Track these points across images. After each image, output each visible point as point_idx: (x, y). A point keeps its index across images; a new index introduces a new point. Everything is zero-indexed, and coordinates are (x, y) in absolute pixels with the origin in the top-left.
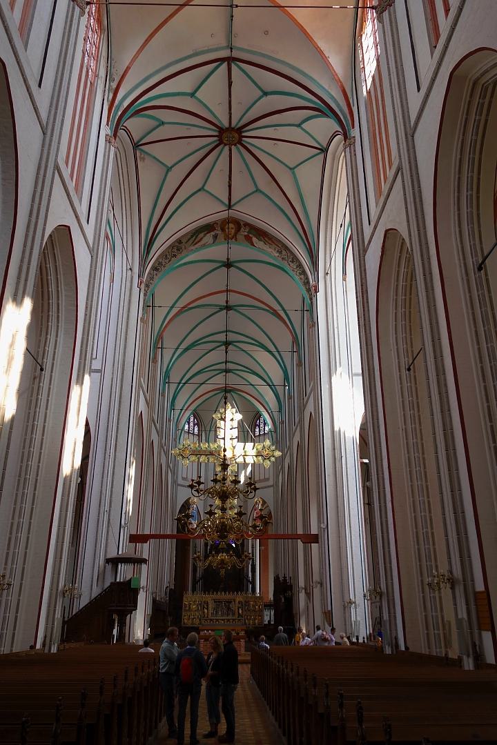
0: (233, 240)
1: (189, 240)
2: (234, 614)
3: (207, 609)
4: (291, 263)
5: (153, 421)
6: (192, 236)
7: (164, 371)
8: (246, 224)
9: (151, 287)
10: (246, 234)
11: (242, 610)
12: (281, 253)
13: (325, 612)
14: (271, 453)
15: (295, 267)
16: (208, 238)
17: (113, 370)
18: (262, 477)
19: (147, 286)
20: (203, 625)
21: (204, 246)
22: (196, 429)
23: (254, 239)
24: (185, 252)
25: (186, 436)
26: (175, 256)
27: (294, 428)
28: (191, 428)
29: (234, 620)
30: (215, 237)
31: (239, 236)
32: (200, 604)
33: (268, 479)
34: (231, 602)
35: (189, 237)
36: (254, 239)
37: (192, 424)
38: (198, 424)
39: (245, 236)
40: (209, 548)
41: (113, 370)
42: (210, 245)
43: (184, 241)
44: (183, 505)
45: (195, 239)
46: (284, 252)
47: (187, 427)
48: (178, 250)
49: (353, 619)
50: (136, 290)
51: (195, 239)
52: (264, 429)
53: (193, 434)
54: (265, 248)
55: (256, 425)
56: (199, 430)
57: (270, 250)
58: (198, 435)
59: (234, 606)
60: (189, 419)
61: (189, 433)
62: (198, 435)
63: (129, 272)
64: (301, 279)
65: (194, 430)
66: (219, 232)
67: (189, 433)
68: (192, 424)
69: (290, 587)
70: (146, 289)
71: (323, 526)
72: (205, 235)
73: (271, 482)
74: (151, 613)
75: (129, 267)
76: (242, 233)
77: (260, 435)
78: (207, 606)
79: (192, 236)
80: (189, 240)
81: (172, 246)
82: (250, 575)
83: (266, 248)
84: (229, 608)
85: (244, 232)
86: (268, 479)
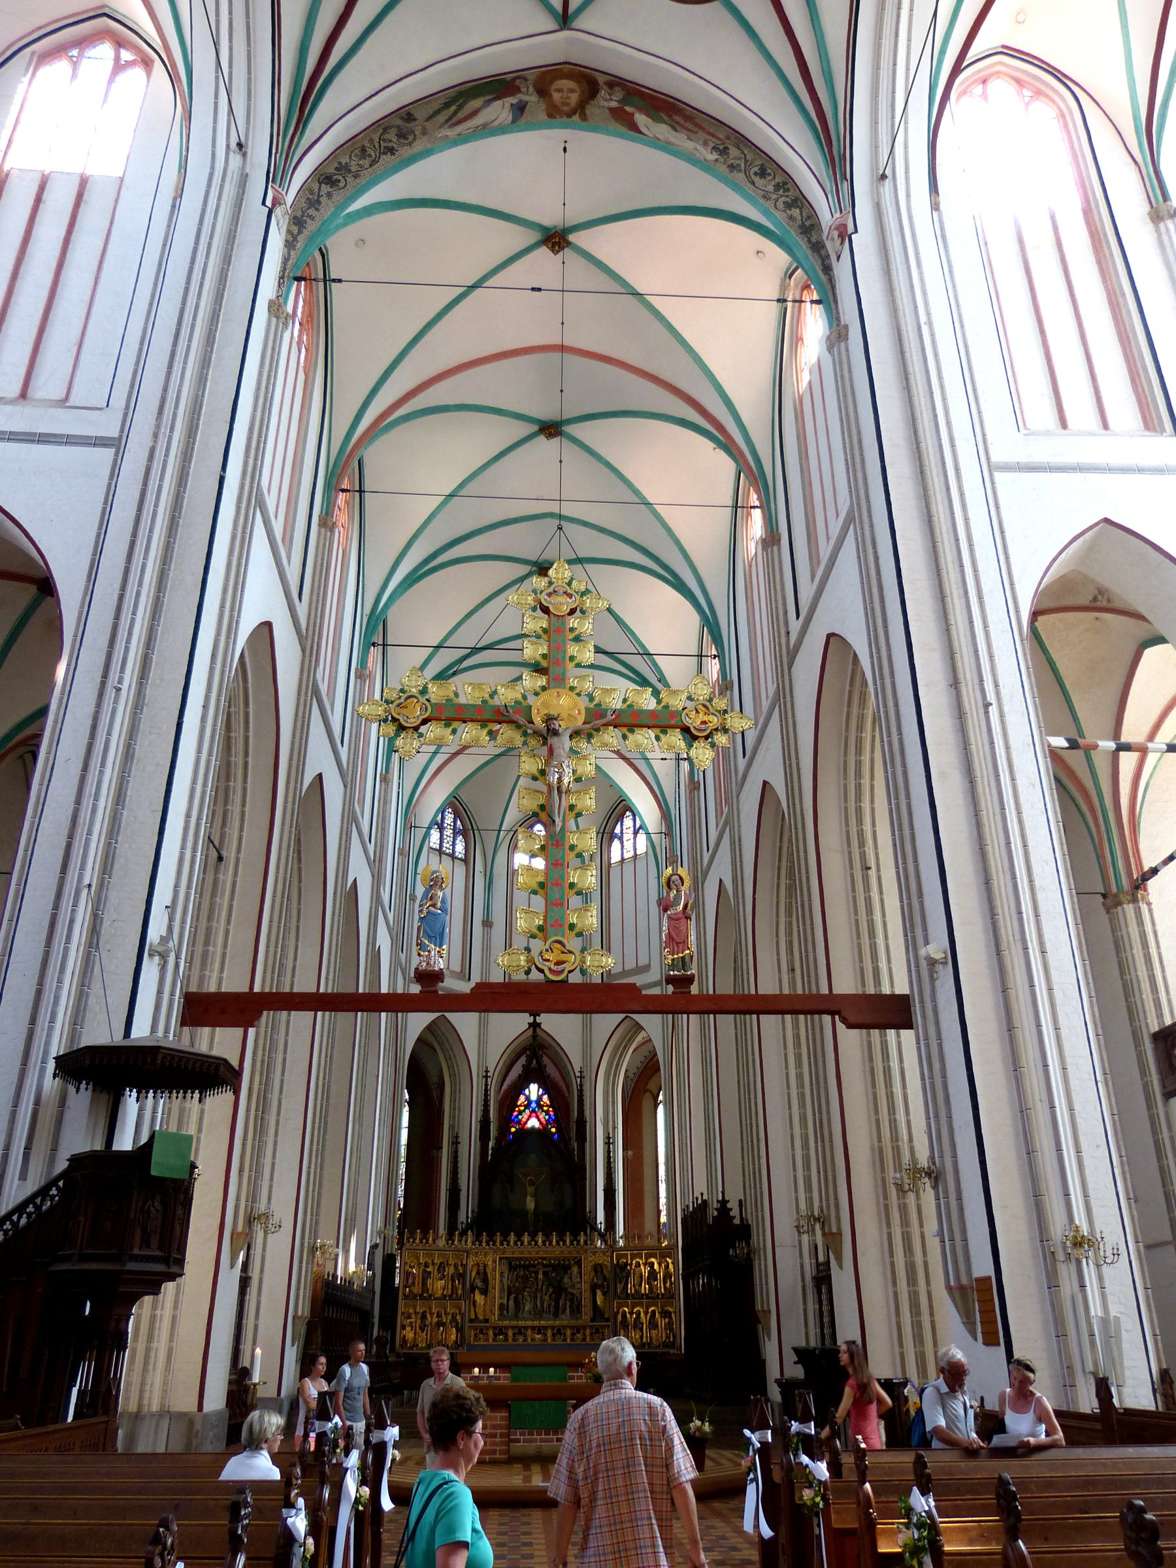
0: (576, 118)
1: (437, 113)
2: (576, 1310)
3: (485, 1292)
4: (757, 179)
5: (316, 693)
6: (447, 105)
7: (367, 610)
8: (616, 82)
9: (311, 226)
10: (614, 104)
11: (605, 1294)
12: (724, 152)
13: (962, 1288)
14: (715, 721)
15: (771, 188)
16: (500, 111)
17: (158, 426)
19: (298, 222)
20: (471, 1348)
21: (487, 130)
22: (460, 848)
23: (641, 119)
24: (418, 146)
25: (435, 858)
26: (391, 151)
27: (742, 763)
28: (447, 846)
29: (578, 1329)
30: (520, 109)
31: (590, 110)
32: (462, 1276)
33: (647, 968)
34: (566, 1268)
35: (436, 106)
36: (641, 119)
38: (464, 833)
39: (612, 110)
40: (491, 1144)
41: (158, 426)
42: (502, 130)
43: (421, 114)
44: (420, 1040)
45: (456, 112)
46: (734, 152)
47: (435, 836)
48: (402, 135)
49: (1096, 1310)
50: (255, 212)
51: (456, 112)
53: (452, 856)
54: (673, 140)
55: (612, 836)
56: (466, 848)
57: (690, 145)
58: (465, 861)
59: (581, 1282)
60: (443, 818)
61: (440, 851)
62: (465, 861)
63: (235, 160)
64: (791, 218)
65: (454, 845)
66: (532, 98)
67: (440, 851)
68: (448, 832)
69: (744, 1231)
70: (295, 229)
71: (936, 948)
72: (487, 103)
74: (307, 1313)
75: (234, 141)
76: (603, 103)
78: (485, 1280)
79: (447, 105)
80: (437, 113)
81: (382, 125)
82: (601, 1216)
83: (680, 139)
84: (559, 1290)
85: (607, 100)
86: (647, 968)
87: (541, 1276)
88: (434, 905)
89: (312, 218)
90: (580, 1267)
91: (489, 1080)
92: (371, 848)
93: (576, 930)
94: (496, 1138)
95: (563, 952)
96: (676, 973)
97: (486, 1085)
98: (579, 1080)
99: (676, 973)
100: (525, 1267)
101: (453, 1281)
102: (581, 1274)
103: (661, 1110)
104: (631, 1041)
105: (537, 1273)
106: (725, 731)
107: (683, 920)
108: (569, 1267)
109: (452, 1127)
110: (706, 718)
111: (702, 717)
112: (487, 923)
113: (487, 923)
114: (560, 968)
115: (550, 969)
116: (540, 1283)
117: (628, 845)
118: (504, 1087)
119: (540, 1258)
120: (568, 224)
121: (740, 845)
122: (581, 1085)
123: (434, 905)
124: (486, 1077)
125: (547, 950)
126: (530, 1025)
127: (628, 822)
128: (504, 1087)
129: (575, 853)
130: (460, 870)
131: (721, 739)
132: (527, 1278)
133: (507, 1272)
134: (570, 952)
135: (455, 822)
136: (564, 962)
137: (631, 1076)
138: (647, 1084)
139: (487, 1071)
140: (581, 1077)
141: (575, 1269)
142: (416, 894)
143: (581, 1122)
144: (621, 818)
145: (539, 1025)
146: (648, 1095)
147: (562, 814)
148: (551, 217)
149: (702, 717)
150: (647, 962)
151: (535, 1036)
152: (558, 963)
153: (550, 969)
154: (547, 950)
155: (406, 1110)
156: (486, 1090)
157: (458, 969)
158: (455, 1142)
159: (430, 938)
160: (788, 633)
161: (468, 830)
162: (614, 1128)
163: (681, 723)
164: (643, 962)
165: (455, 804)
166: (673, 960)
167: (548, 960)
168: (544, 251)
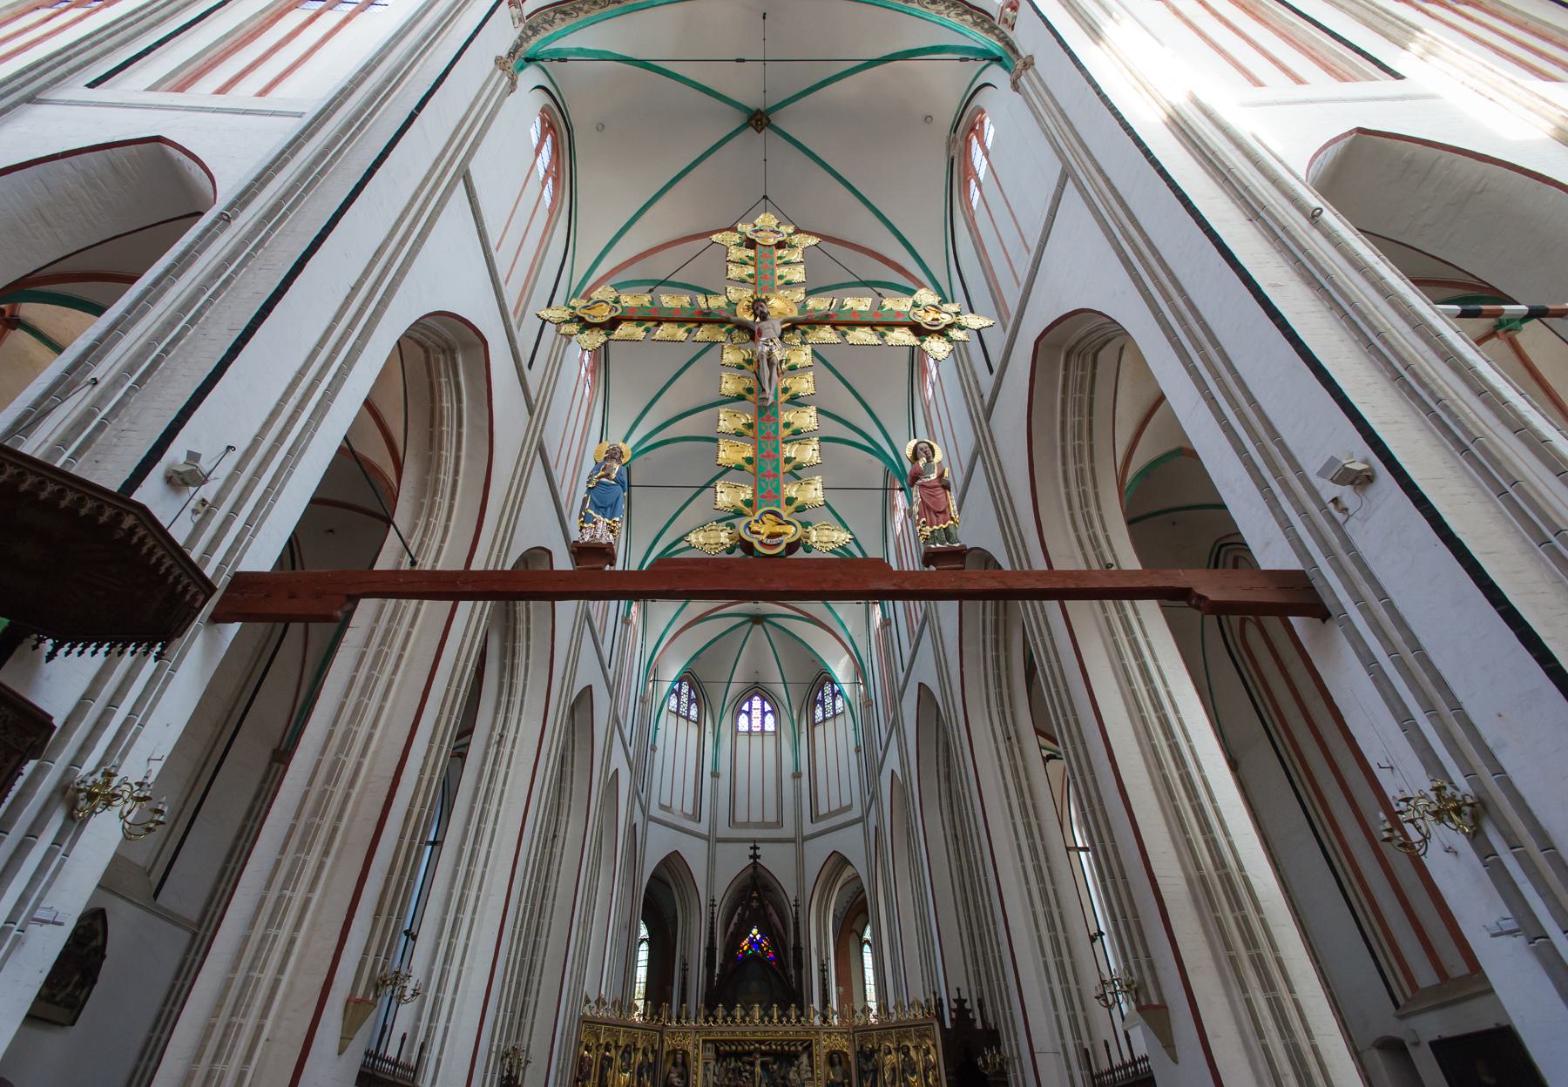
4: (929, 6)
5: (541, 449)
14: (947, 319)
15: (942, 8)
18: (835, 806)
22: (694, 712)
25: (672, 718)
28: (683, 710)
33: (850, 807)
37: (684, 699)
38: (697, 701)
44: (654, 876)
52: (834, 706)
53: (687, 718)
55: (816, 702)
56: (699, 713)
60: (680, 687)
61: (677, 714)
62: (698, 723)
65: (689, 709)
68: (684, 699)
73: (856, 812)
77: (825, 719)
86: (850, 807)
87: (758, 1069)
88: (607, 476)
89: (545, 29)
90: (810, 1056)
91: (716, 909)
92: (611, 672)
93: (796, 504)
94: (721, 965)
95: (779, 524)
96: (938, 545)
97: (713, 913)
98: (794, 909)
99: (938, 545)
100: (738, 1056)
101: (640, 1075)
102: (812, 1066)
103: (867, 948)
104: (839, 874)
105: (752, 1064)
106: (962, 328)
107: (941, 490)
108: (797, 1056)
109: (683, 957)
110: (936, 316)
111: (932, 315)
112: (715, 775)
113: (715, 775)
114: (775, 541)
115: (761, 542)
116: (757, 1080)
117: (829, 707)
118: (729, 933)
119: (757, 1041)
120: (769, 106)
121: (940, 634)
122: (797, 913)
123: (607, 476)
124: (713, 906)
125: (756, 521)
126: (751, 857)
127: (828, 689)
128: (729, 933)
129: (790, 429)
130: (694, 729)
131: (956, 334)
132: (740, 1072)
133: (713, 1063)
134: (789, 523)
135: (690, 692)
136: (779, 535)
137: (839, 915)
138: (852, 924)
139: (713, 900)
140: (796, 906)
141: (804, 1059)
142: (657, 745)
143: (798, 949)
144: (821, 688)
145: (759, 857)
146: (854, 935)
147: (773, 388)
148: (754, 101)
149: (932, 315)
150: (849, 803)
151: (755, 865)
152: (771, 536)
153: (761, 542)
154: (756, 521)
155: (644, 946)
156: (713, 918)
157: (691, 813)
158: (685, 969)
159: (597, 508)
160: (982, 396)
161: (701, 697)
162: (828, 958)
163: (908, 320)
164: (846, 802)
165: (688, 676)
166: (932, 532)
167: (758, 533)
168: (751, 131)
